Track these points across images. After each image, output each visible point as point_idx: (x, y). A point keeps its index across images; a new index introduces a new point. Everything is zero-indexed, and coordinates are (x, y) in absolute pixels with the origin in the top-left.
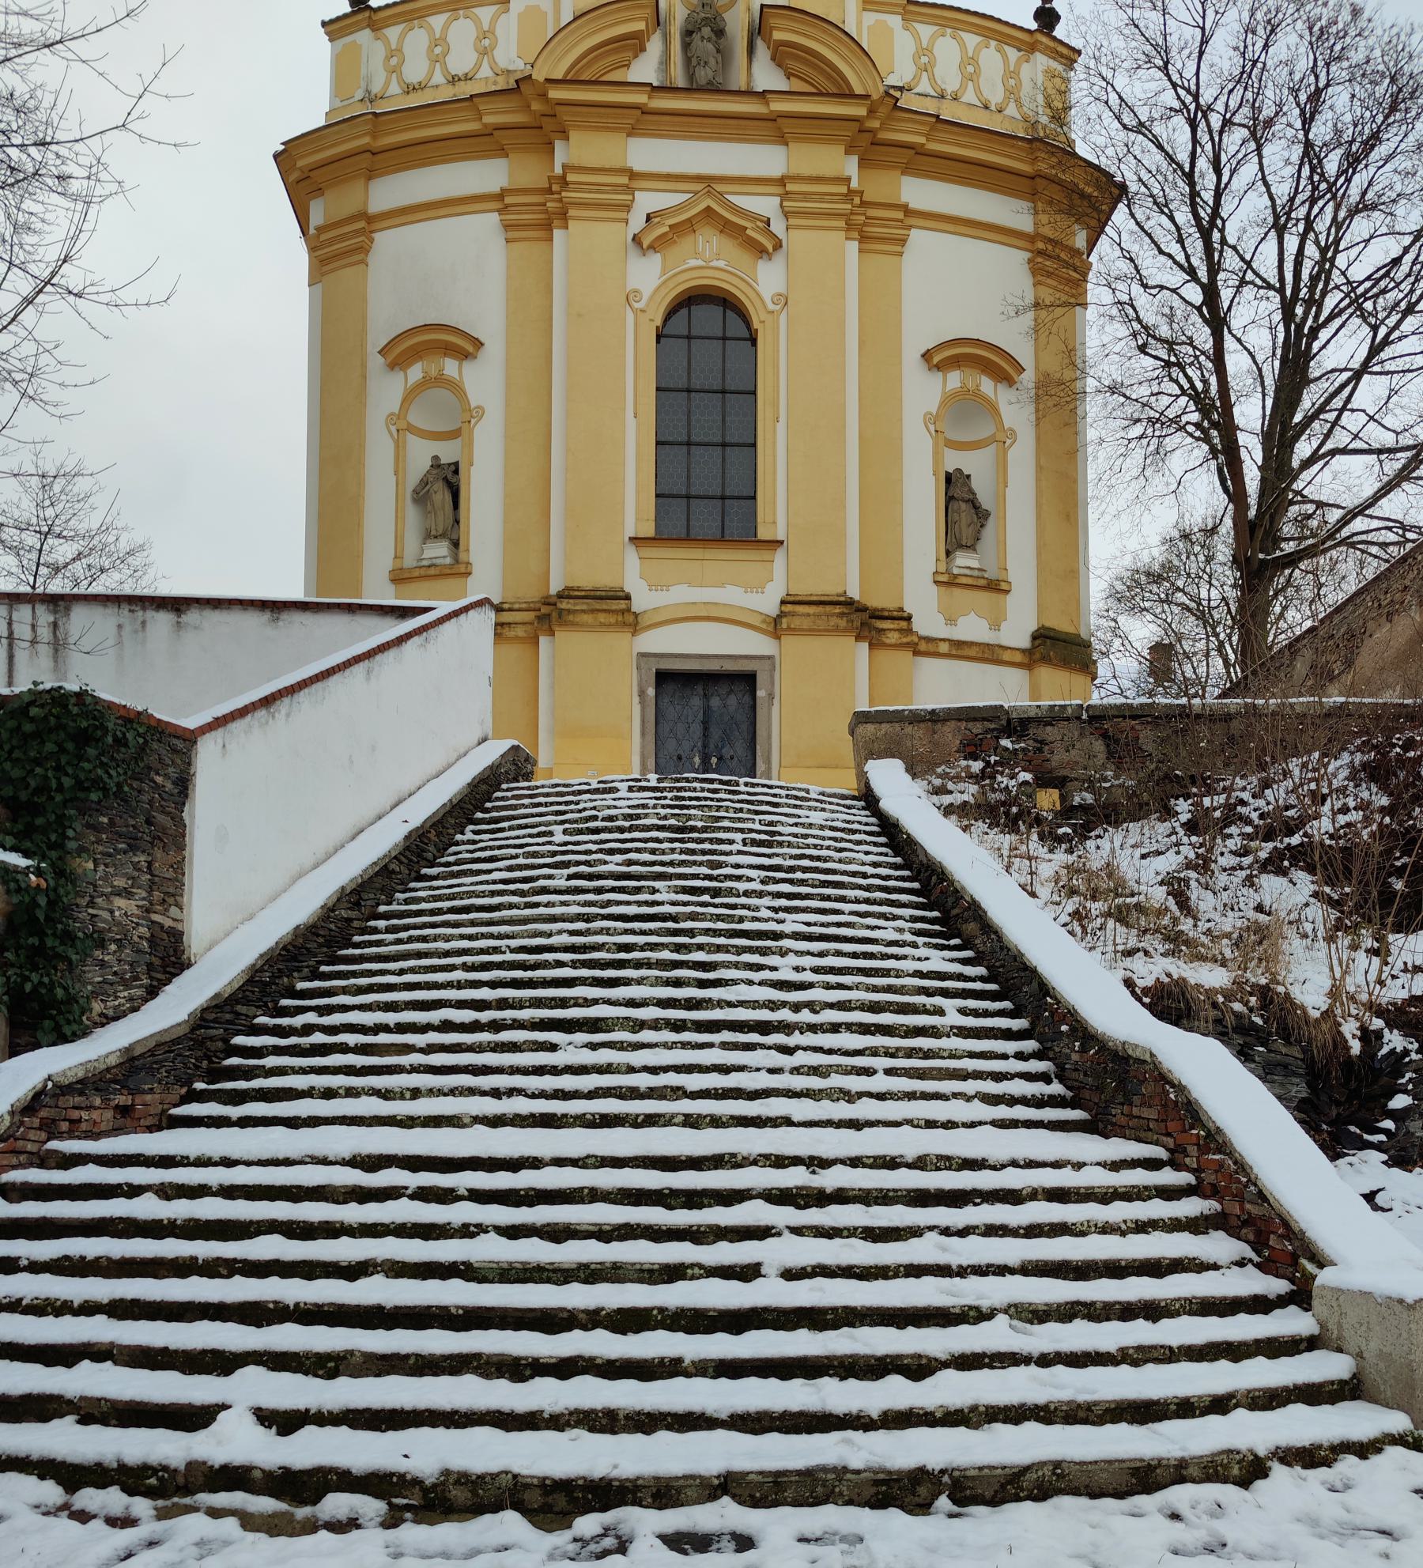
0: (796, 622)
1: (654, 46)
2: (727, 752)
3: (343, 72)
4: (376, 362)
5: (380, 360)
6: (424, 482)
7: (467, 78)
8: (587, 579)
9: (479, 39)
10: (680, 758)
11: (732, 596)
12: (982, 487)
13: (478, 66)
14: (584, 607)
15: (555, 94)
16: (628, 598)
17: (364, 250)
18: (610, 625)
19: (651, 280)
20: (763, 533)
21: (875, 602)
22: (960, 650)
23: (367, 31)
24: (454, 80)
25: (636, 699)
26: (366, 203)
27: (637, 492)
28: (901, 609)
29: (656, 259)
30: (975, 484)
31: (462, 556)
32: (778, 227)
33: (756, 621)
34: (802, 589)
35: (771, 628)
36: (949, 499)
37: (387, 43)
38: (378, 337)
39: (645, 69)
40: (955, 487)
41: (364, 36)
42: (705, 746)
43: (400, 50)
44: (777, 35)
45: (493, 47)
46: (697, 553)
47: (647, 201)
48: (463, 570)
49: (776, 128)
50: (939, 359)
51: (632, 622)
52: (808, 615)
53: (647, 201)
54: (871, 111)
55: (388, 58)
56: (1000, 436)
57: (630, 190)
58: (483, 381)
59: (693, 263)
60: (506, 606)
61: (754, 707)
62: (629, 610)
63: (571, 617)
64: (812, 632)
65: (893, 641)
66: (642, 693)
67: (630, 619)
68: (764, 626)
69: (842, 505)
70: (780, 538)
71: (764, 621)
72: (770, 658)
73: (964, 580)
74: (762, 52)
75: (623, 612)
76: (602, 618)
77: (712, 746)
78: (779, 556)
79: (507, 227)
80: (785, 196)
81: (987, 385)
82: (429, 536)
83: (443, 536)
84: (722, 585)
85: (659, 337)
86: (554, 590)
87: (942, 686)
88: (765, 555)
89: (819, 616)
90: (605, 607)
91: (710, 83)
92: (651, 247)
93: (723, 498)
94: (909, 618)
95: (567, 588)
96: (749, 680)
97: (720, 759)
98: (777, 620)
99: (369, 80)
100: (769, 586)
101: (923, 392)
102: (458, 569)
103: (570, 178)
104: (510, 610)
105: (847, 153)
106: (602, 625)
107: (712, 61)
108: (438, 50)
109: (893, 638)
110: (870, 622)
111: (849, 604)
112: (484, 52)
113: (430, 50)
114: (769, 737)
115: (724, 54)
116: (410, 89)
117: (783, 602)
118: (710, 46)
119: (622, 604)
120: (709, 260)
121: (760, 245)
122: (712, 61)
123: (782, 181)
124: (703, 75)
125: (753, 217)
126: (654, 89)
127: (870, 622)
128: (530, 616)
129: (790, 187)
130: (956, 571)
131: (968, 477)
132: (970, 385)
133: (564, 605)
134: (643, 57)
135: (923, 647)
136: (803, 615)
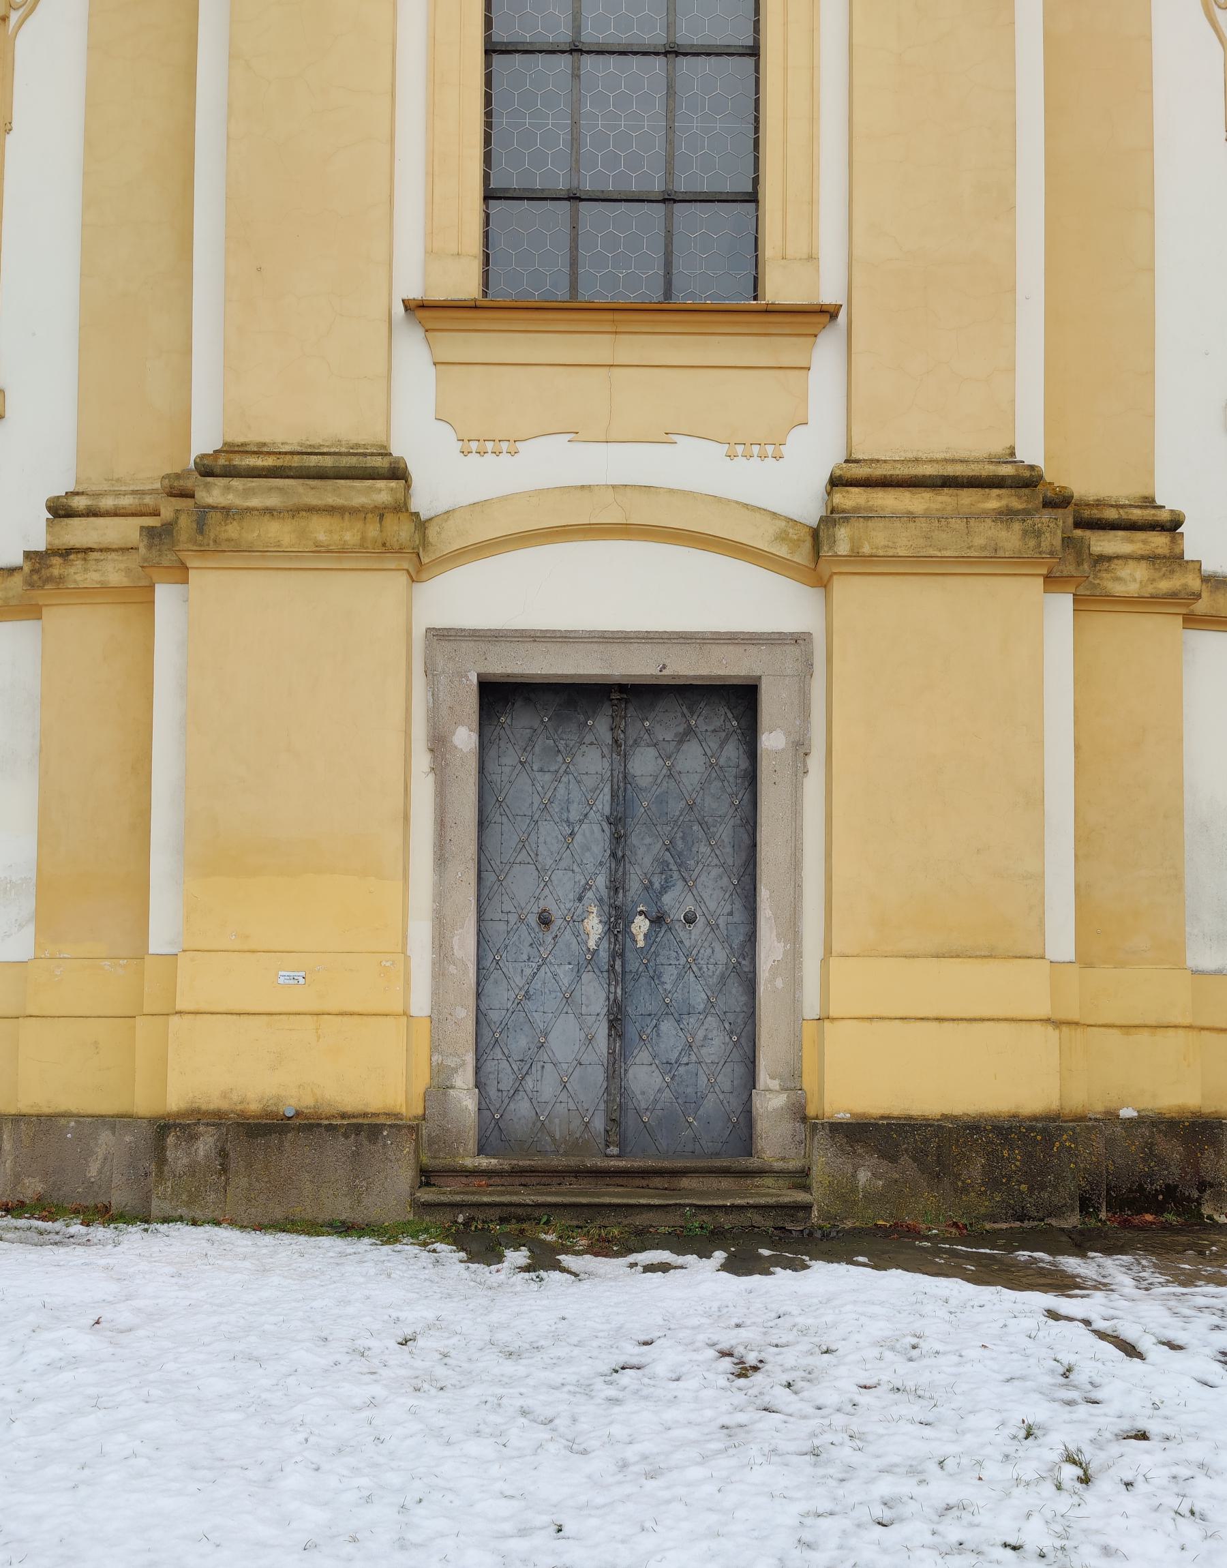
0: (877, 538)
2: (676, 902)
8: (284, 425)
10: (545, 920)
11: (693, 467)
14: (273, 501)
16: (398, 473)
18: (343, 551)
20: (780, 288)
21: (1088, 481)
25: (422, 761)
27: (431, 176)
28: (1149, 502)
33: (759, 536)
35: (802, 556)
42: (616, 886)
46: (593, 345)
51: (413, 545)
52: (911, 517)
60: (80, 503)
61: (751, 778)
62: (401, 507)
63: (232, 530)
64: (921, 565)
65: (1132, 589)
66: (438, 744)
67: (402, 531)
68: (782, 551)
69: (1003, 204)
70: (829, 295)
71: (782, 537)
72: (799, 640)
75: (380, 513)
76: (321, 530)
77: (634, 886)
84: (667, 438)
88: (785, 350)
89: (941, 518)
90: (331, 500)
93: (668, 199)
94: (1172, 526)
95: (230, 449)
96: (741, 699)
97: (658, 920)
98: (817, 537)
100: (797, 437)
104: (92, 513)
106: (320, 550)
109: (1132, 579)
114: (796, 864)
117: (836, 482)
119: (382, 492)
133: (216, 493)
136: (895, 517)
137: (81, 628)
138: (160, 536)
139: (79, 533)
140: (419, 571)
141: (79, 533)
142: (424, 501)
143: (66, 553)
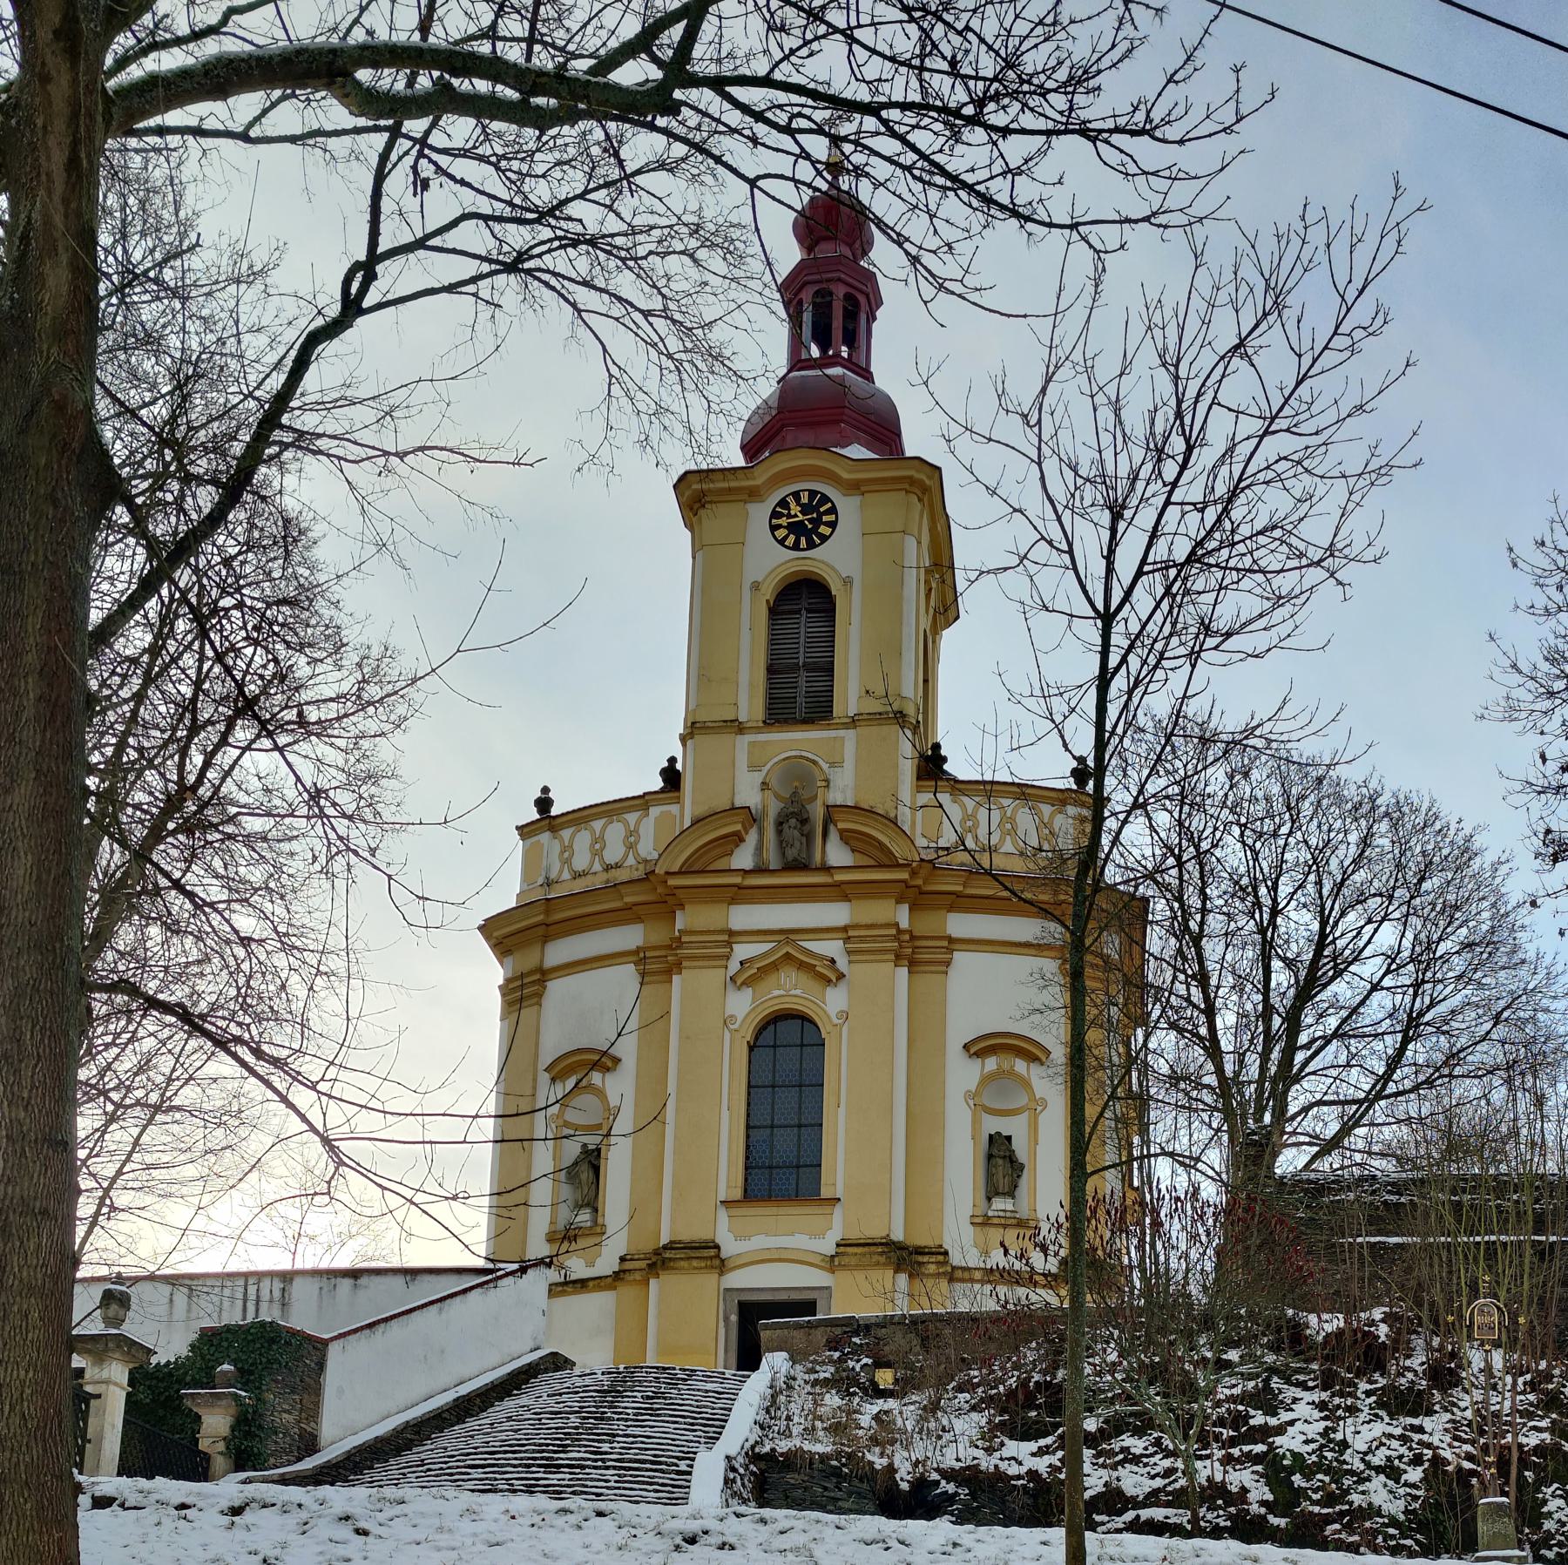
0: (845, 1260)
1: (752, 838)
3: (530, 862)
4: (544, 1078)
5: (547, 1075)
6: (576, 1163)
7: (617, 866)
8: (686, 1236)
9: (627, 837)
11: (801, 1241)
12: (1020, 1147)
13: (626, 856)
15: (672, 882)
16: (717, 1247)
17: (539, 995)
19: (743, 1007)
20: (825, 1192)
23: (548, 834)
24: (608, 868)
25: (722, 1324)
26: (542, 961)
29: (748, 993)
30: (1015, 1144)
31: (600, 1220)
32: (842, 964)
33: (817, 1260)
34: (854, 1235)
37: (562, 841)
38: (546, 1059)
39: (743, 858)
41: (545, 837)
43: (571, 846)
44: (841, 825)
45: (637, 842)
46: (774, 1210)
47: (743, 951)
48: (598, 1230)
49: (841, 892)
50: (980, 1048)
53: (743, 951)
54: (914, 873)
55: (562, 852)
56: (1032, 1105)
57: (729, 944)
58: (619, 1087)
59: (777, 993)
62: (718, 1256)
64: (858, 1267)
66: (726, 1319)
67: (717, 1262)
73: (996, 1221)
74: (834, 836)
75: (711, 1258)
76: (695, 1263)
78: (838, 1210)
79: (643, 974)
80: (847, 940)
81: (1020, 1066)
82: (579, 1206)
83: (588, 1205)
84: (792, 1234)
85: (751, 1048)
86: (664, 1240)
88: (827, 1209)
89: (864, 1255)
91: (795, 860)
92: (743, 983)
99: (548, 870)
101: (963, 1075)
102: (597, 1230)
103: (684, 939)
105: (898, 902)
107: (797, 844)
108: (597, 846)
109: (932, 1268)
112: (631, 847)
113: (592, 846)
115: (809, 838)
116: (577, 875)
118: (796, 833)
119: (712, 1252)
120: (789, 990)
121: (828, 975)
122: (797, 844)
123: (845, 929)
124: (791, 853)
125: (821, 958)
126: (745, 872)
128: (643, 1264)
129: (851, 933)
130: (990, 1214)
131: (1009, 1138)
132: (1006, 1066)
133: (668, 1255)
134: (743, 845)
135: (959, 1274)
137: (627, 1291)
138: (652, 1266)
139: (628, 1265)
140: (721, 1274)
141: (628, 1265)
142: (723, 1255)
143: (624, 1271)
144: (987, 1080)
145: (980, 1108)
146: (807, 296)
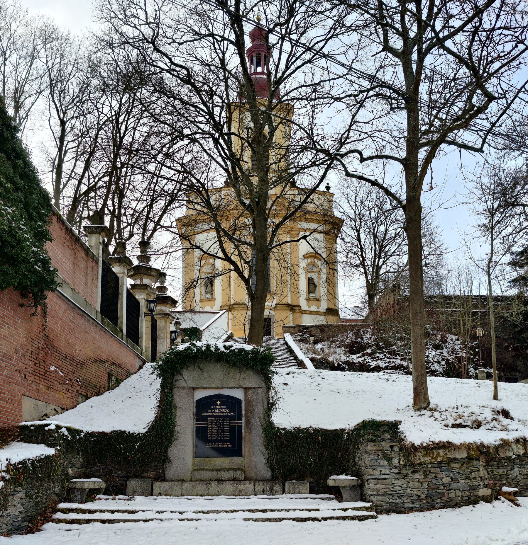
22: (311, 313)
36: (309, 283)
40: (310, 281)
82: (206, 293)
87: (307, 320)
102: (213, 299)
109: (297, 311)
110: (293, 308)
111: (289, 305)
127: (293, 308)
144: (308, 264)
145: (307, 272)
146: (254, 54)
